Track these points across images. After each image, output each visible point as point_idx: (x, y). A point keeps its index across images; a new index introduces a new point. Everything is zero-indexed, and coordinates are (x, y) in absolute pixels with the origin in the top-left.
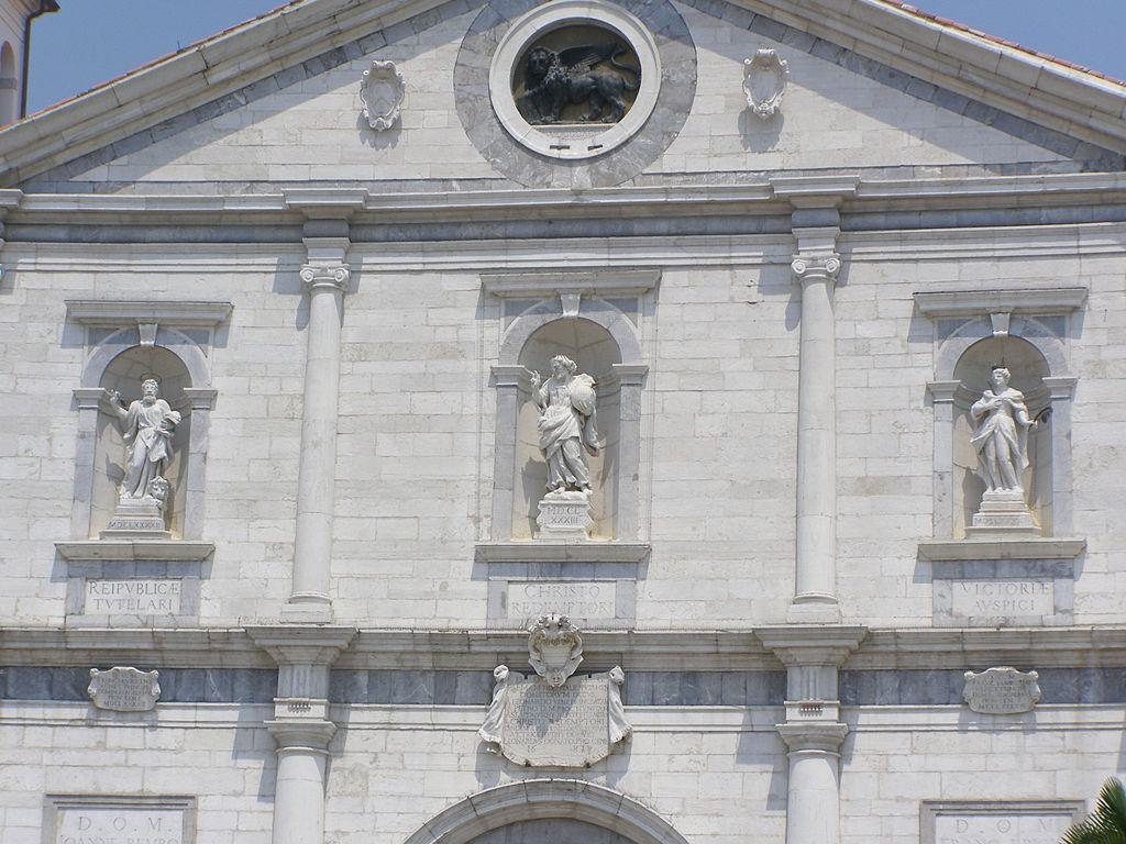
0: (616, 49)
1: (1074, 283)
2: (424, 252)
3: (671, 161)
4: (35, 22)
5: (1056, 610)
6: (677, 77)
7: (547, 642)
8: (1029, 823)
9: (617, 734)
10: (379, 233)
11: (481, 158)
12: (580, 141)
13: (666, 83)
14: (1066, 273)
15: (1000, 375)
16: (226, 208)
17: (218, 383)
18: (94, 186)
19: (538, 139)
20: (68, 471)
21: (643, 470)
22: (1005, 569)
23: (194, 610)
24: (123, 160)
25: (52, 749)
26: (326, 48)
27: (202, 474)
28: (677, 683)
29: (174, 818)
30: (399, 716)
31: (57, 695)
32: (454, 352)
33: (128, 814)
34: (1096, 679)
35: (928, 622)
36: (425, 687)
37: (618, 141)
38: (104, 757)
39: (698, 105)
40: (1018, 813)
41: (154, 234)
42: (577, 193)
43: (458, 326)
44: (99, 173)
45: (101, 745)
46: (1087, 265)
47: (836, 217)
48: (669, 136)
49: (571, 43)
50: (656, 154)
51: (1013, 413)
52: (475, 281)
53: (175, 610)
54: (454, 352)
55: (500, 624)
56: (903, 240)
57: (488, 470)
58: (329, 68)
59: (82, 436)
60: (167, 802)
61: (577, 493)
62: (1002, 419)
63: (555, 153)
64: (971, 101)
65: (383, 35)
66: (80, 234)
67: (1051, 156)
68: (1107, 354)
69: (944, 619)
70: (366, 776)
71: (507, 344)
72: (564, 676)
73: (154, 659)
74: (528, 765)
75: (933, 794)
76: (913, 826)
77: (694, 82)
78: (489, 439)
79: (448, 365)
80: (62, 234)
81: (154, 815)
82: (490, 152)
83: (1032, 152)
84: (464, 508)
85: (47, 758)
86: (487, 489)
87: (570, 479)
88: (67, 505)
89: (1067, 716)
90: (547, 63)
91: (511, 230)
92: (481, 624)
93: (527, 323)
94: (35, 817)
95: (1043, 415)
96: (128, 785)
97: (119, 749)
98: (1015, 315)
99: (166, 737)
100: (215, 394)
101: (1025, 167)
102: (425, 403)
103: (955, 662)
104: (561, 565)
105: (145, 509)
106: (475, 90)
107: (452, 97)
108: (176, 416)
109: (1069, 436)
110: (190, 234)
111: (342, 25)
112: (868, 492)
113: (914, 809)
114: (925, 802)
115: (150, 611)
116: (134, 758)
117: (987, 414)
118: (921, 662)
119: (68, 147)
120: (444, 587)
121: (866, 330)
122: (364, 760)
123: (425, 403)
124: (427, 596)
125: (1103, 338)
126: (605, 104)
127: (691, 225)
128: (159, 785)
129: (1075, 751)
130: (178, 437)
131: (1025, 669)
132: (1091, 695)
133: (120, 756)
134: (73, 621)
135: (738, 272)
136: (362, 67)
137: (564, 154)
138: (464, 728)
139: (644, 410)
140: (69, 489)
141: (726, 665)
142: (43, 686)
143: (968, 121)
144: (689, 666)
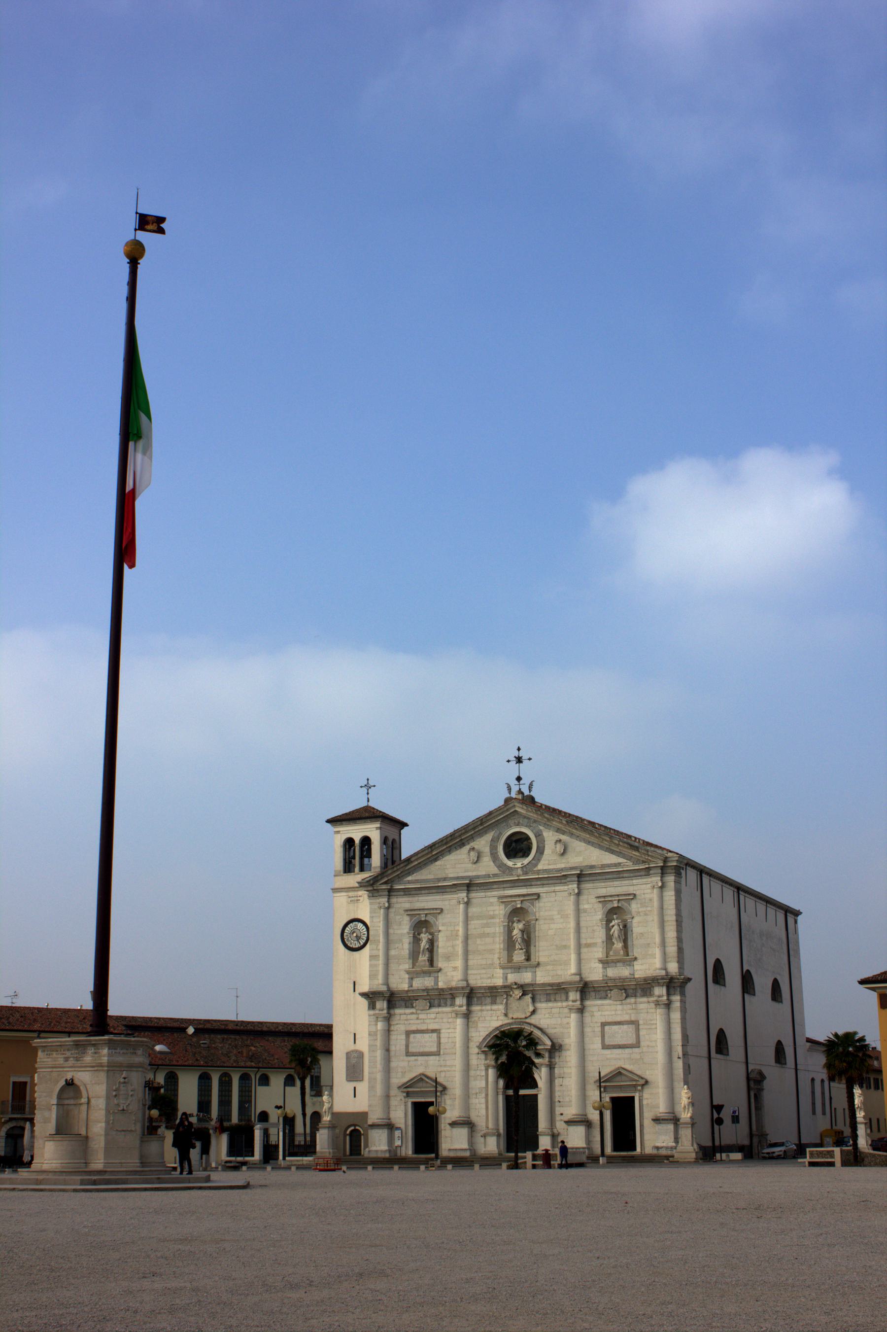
0: (528, 838)
1: (632, 892)
2: (485, 892)
3: (540, 867)
4: (402, 831)
5: (630, 974)
6: (541, 845)
7: (514, 988)
8: (625, 1027)
9: (531, 1008)
10: (475, 888)
11: (496, 869)
12: (519, 863)
13: (538, 847)
14: (631, 890)
15: (615, 916)
16: (440, 885)
17: (440, 928)
18: (409, 882)
19: (510, 863)
20: (407, 951)
21: (537, 944)
22: (618, 964)
23: (437, 985)
24: (415, 874)
25: (407, 1020)
26: (459, 844)
27: (438, 951)
28: (545, 996)
29: (435, 1035)
30: (484, 1008)
31: (406, 1007)
32: (493, 917)
33: (425, 1035)
34: (639, 991)
35: (601, 979)
36: (489, 1000)
37: (528, 862)
38: (419, 1021)
39: (545, 852)
40: (623, 1024)
41: (423, 892)
42: (518, 876)
43: (494, 911)
44: (410, 878)
45: (418, 1019)
46: (635, 888)
47: (576, 879)
48: (539, 860)
49: (518, 837)
50: (536, 865)
51: (619, 925)
52: (495, 899)
53: (433, 984)
54: (493, 917)
55: (506, 984)
56: (593, 883)
57: (502, 946)
58: (461, 848)
59: (410, 943)
60: (433, 1031)
61: (521, 951)
62: (616, 927)
63: (513, 866)
64: (607, 848)
65: (472, 838)
66: (407, 893)
67: (626, 861)
68: (640, 910)
69: (605, 978)
70: (477, 1023)
71: (505, 915)
72: (518, 996)
73: (428, 997)
74: (513, 1018)
75: (603, 1021)
76: (599, 1029)
77: (544, 847)
78: (502, 938)
79: (492, 921)
80: (402, 893)
81: (431, 1034)
82: (499, 867)
83: (621, 860)
84: (497, 956)
85: (406, 1022)
86: (502, 951)
87: (520, 947)
88: (407, 960)
89: (632, 1000)
90: (511, 844)
91: (505, 886)
92: (501, 984)
93: (509, 908)
94: (404, 1037)
95: (625, 926)
96: (424, 1027)
97: (421, 1019)
98: (619, 901)
99: (433, 1016)
100: (440, 931)
101: (620, 864)
102: (487, 930)
103: (607, 988)
104: (518, 969)
105: (425, 960)
106: (495, 851)
107: (489, 854)
108: (430, 937)
109: (632, 931)
110: (431, 891)
111: (463, 838)
112: (587, 947)
113: (600, 1024)
114: (602, 1023)
115: (427, 985)
116: (426, 1021)
117: (613, 926)
118: (599, 989)
119: (401, 872)
120: (493, 975)
121: (586, 906)
122: (476, 1019)
123: (487, 930)
124: (490, 978)
125: (639, 906)
126: (526, 852)
127: (545, 882)
128: (432, 1027)
129: (635, 1009)
130: (432, 942)
131: (621, 990)
132: (638, 994)
133: (422, 1021)
134: (411, 988)
135: (557, 893)
136: (467, 847)
137: (516, 866)
138: (499, 1010)
139: (537, 929)
140: (407, 956)
141: (556, 992)
142: (403, 1004)
143: (607, 853)
144: (548, 992)
